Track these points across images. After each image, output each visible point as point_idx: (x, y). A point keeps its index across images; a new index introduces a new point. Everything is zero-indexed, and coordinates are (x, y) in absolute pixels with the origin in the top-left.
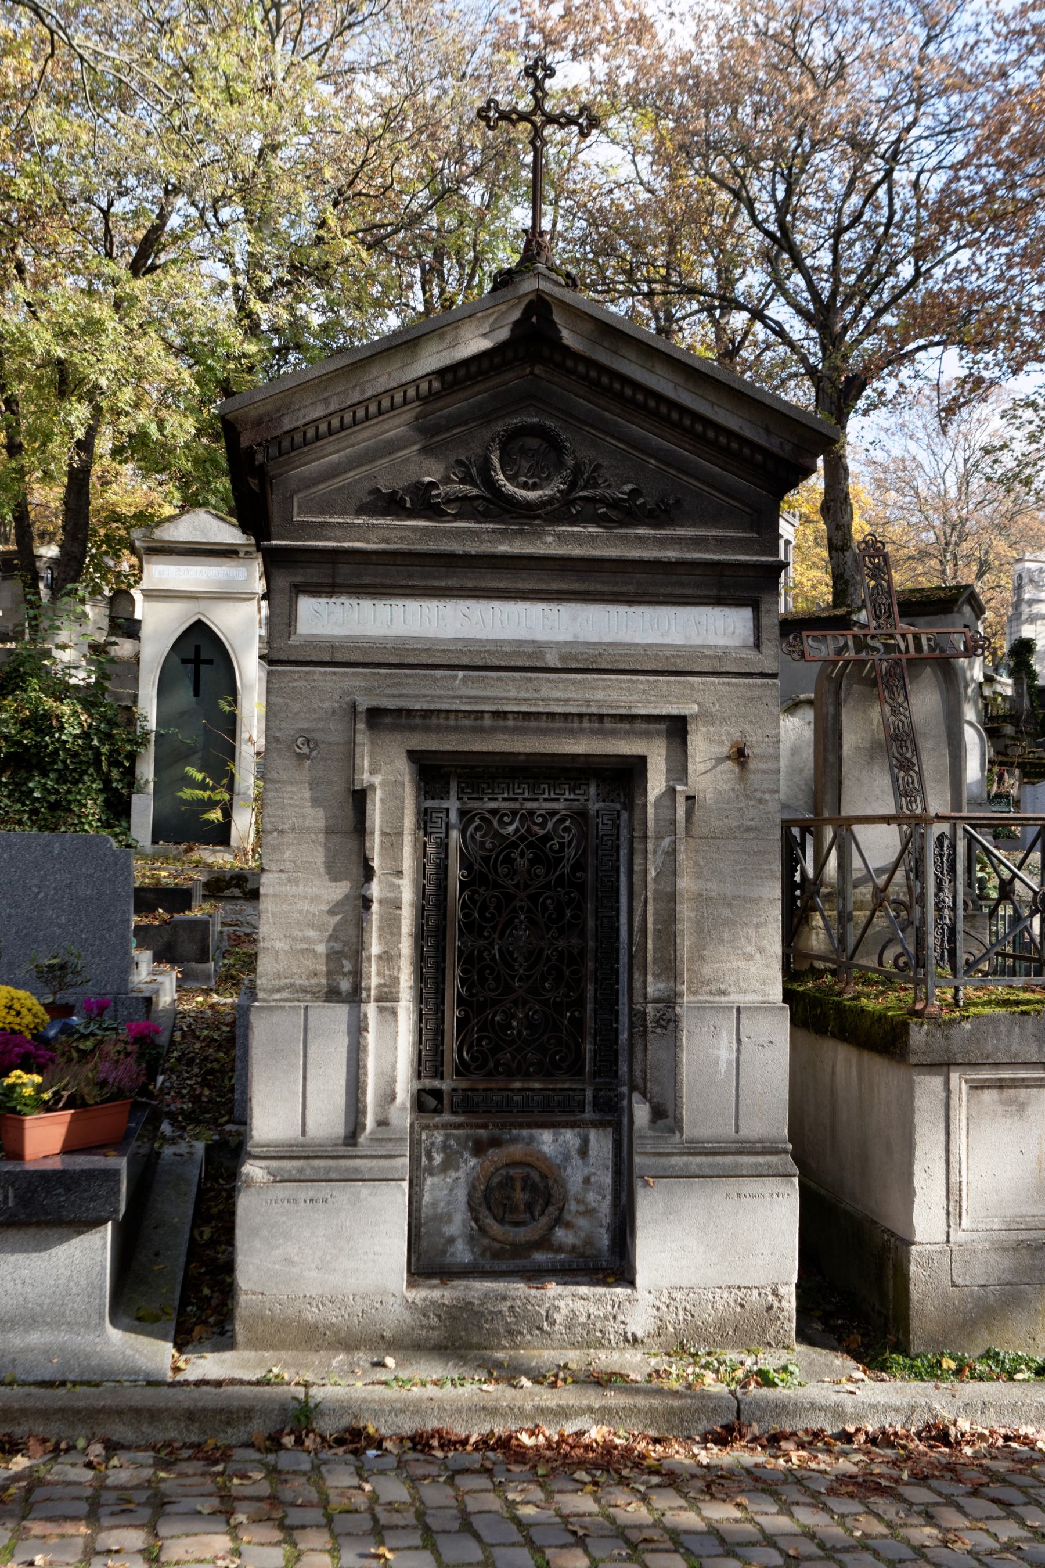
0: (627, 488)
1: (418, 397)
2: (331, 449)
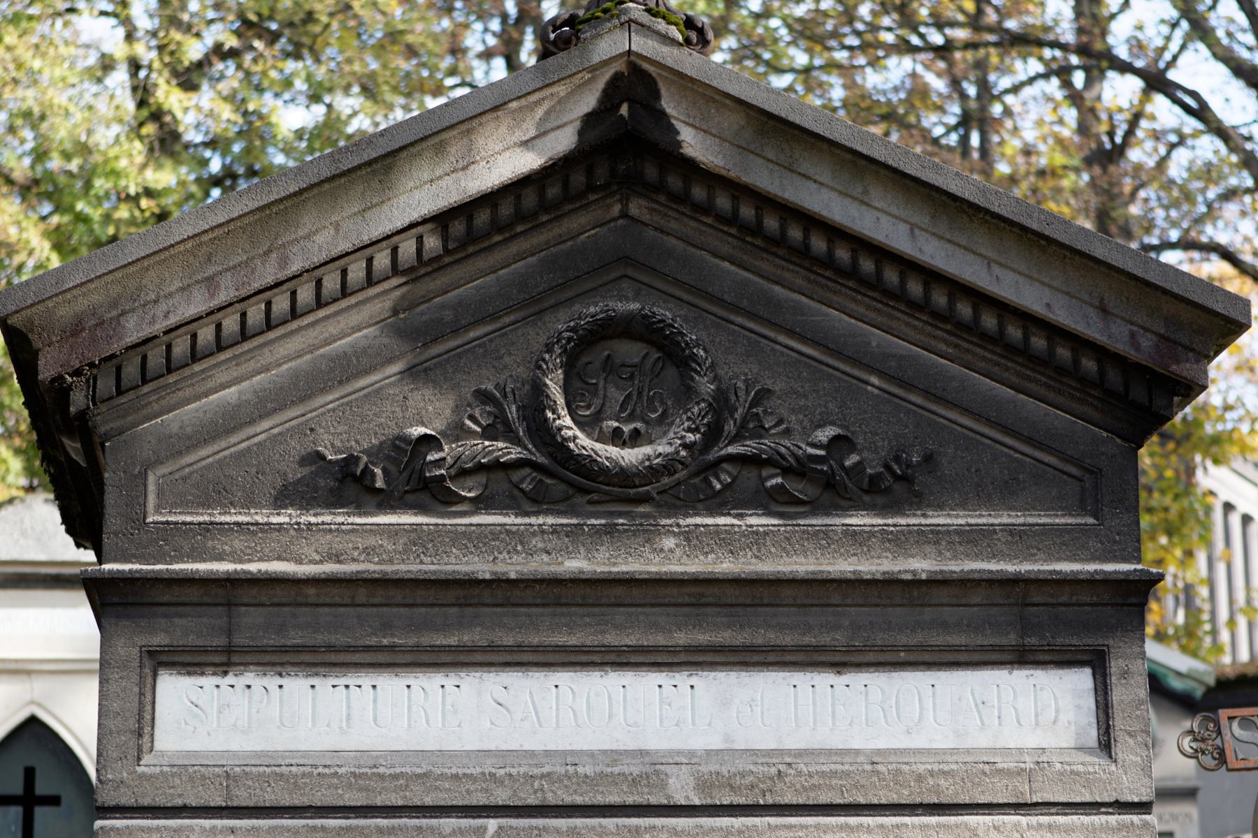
0: (824, 435)
1: (395, 269)
2: (221, 377)
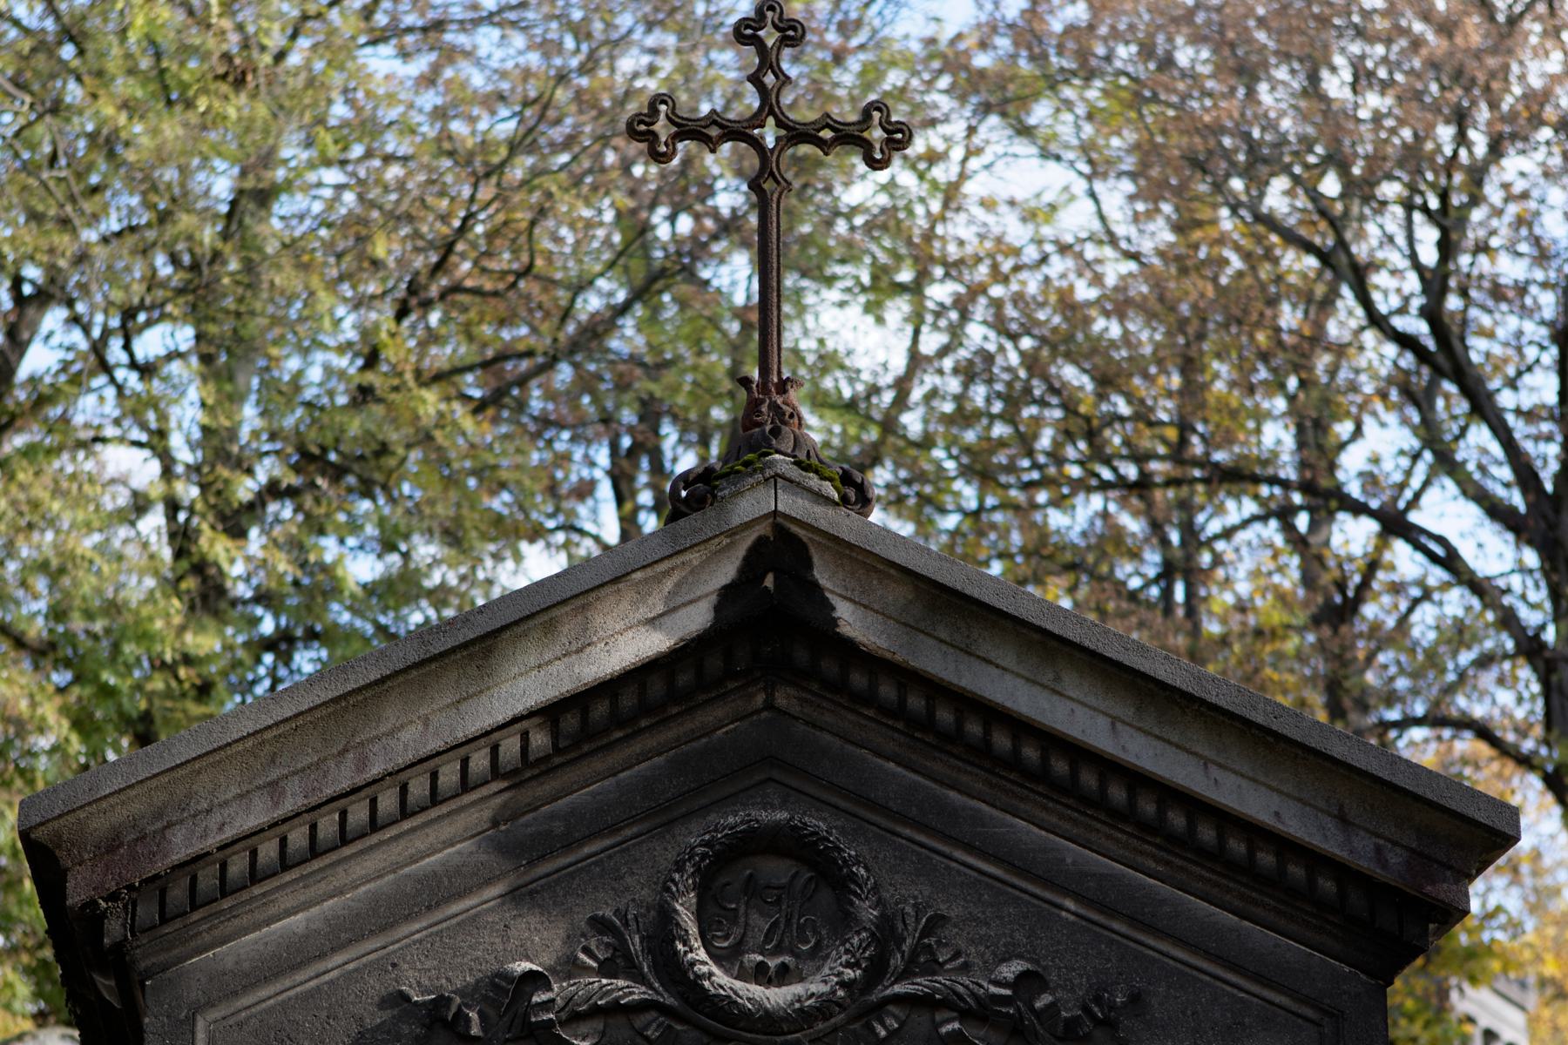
0: (1010, 970)
1: (496, 771)
2: (286, 901)
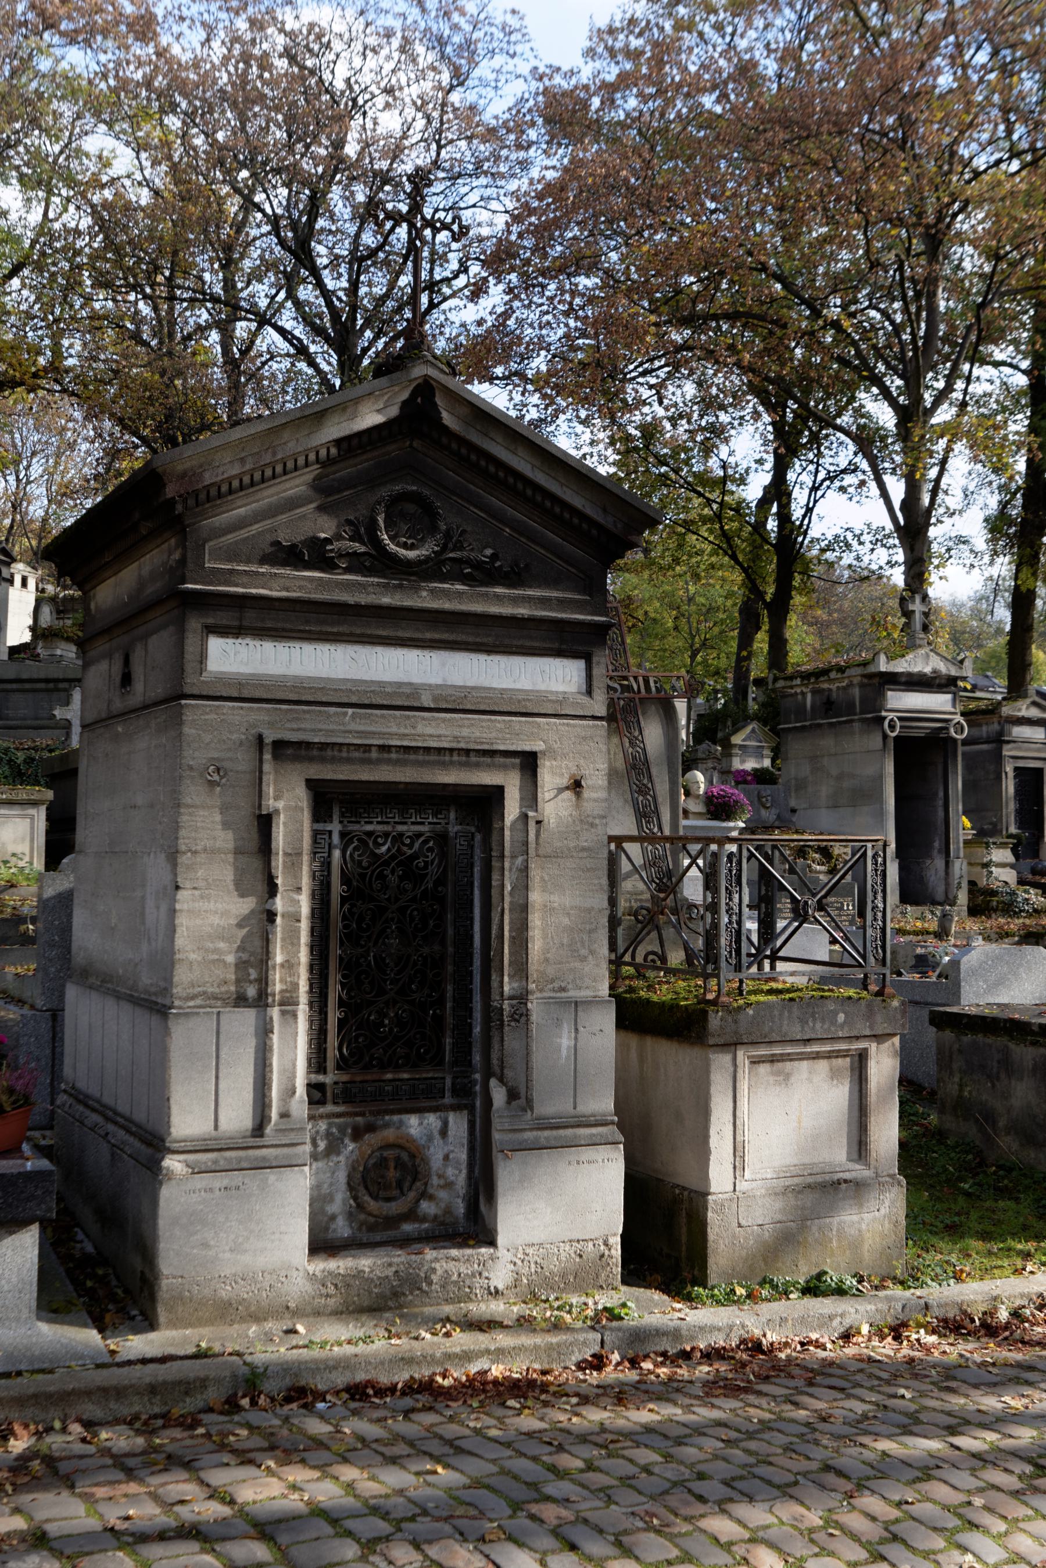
0: (489, 552)
1: (318, 461)
2: (239, 503)
